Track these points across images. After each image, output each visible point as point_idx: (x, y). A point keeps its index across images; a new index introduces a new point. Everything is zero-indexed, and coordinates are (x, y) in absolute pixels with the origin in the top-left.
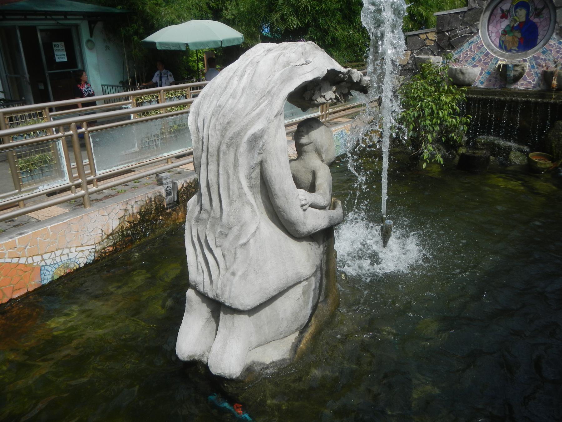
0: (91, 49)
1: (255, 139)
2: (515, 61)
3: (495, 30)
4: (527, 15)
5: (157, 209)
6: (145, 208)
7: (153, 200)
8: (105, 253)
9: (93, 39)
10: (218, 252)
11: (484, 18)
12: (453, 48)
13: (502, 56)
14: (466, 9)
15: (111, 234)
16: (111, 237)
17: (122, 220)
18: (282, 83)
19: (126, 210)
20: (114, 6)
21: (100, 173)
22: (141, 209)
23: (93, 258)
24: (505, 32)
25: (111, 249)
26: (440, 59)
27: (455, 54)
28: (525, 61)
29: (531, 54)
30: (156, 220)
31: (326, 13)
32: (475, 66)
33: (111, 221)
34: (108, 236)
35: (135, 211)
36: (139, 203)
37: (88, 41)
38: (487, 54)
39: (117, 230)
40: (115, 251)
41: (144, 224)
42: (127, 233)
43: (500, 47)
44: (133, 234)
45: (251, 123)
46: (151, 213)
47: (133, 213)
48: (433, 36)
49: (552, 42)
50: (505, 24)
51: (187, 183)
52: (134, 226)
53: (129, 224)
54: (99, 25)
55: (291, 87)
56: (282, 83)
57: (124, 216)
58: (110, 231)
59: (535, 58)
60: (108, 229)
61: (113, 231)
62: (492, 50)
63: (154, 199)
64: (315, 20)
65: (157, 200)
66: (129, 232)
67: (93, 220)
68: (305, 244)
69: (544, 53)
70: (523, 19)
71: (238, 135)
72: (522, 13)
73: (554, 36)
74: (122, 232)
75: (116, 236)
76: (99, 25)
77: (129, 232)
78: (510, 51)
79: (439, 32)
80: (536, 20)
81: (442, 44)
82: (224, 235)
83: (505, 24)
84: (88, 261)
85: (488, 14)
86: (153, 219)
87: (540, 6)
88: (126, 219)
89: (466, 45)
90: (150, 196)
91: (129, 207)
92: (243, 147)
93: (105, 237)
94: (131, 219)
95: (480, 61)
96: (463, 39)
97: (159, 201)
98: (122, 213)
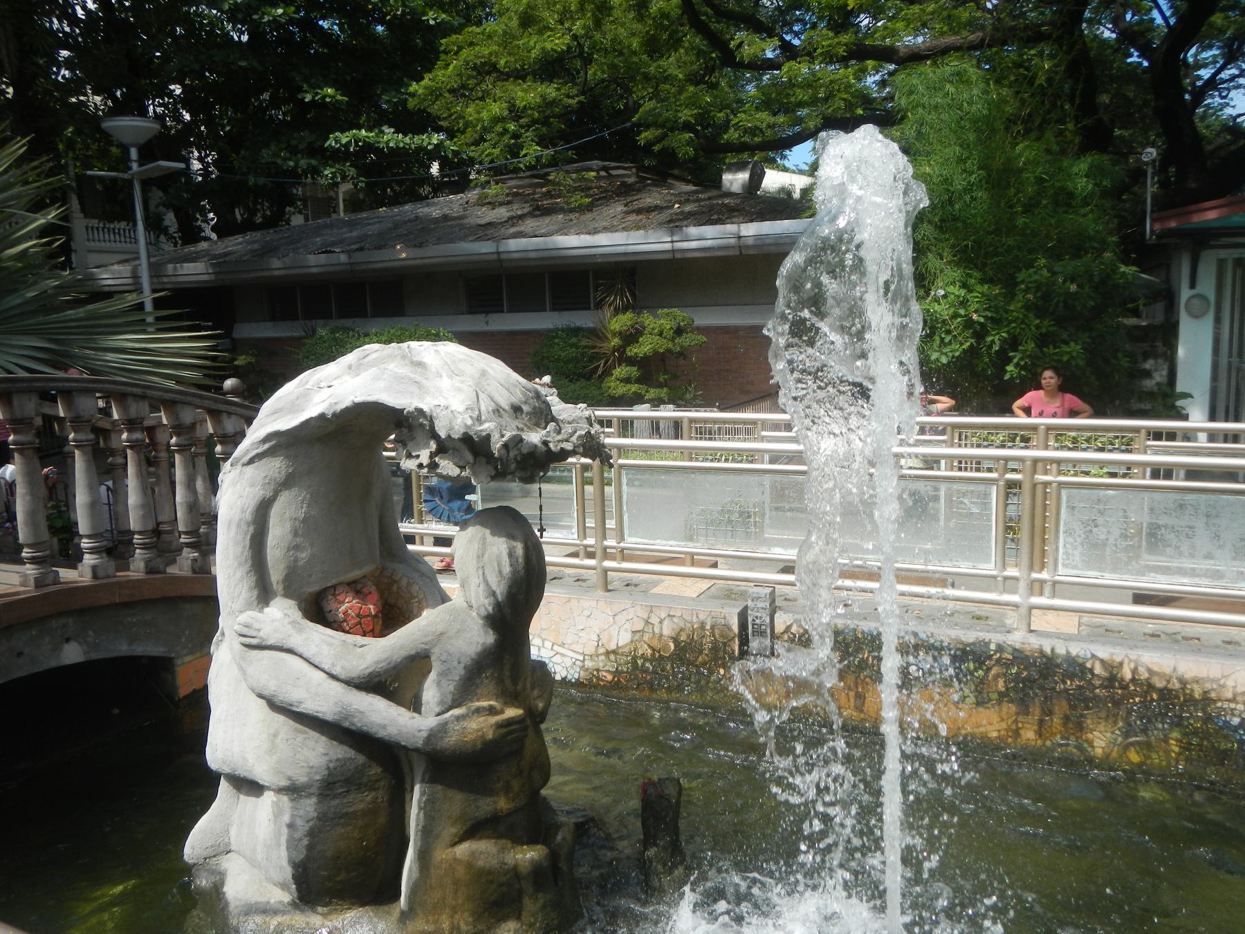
5: (715, 649)
6: (688, 636)
7: (708, 627)
8: (598, 678)
15: (614, 652)
16: (612, 657)
17: (637, 637)
18: (274, 413)
19: (647, 622)
21: (631, 541)
22: (678, 634)
23: (576, 676)
25: (609, 677)
30: (711, 673)
33: (616, 627)
34: (608, 653)
35: (666, 632)
36: (675, 620)
39: (626, 650)
40: (615, 685)
41: (683, 665)
42: (643, 665)
44: (654, 672)
46: (701, 652)
47: (661, 635)
51: (800, 626)
52: (658, 658)
53: (650, 651)
56: (274, 413)
57: (643, 631)
58: (613, 647)
60: (610, 640)
61: (618, 648)
63: (713, 627)
65: (717, 632)
66: (648, 665)
67: (586, 613)
68: (281, 718)
74: (635, 658)
75: (623, 659)
77: (648, 665)
84: (569, 677)
86: (704, 664)
88: (646, 638)
90: (702, 617)
91: (654, 620)
93: (602, 651)
94: (655, 644)
97: (722, 636)
98: (639, 626)
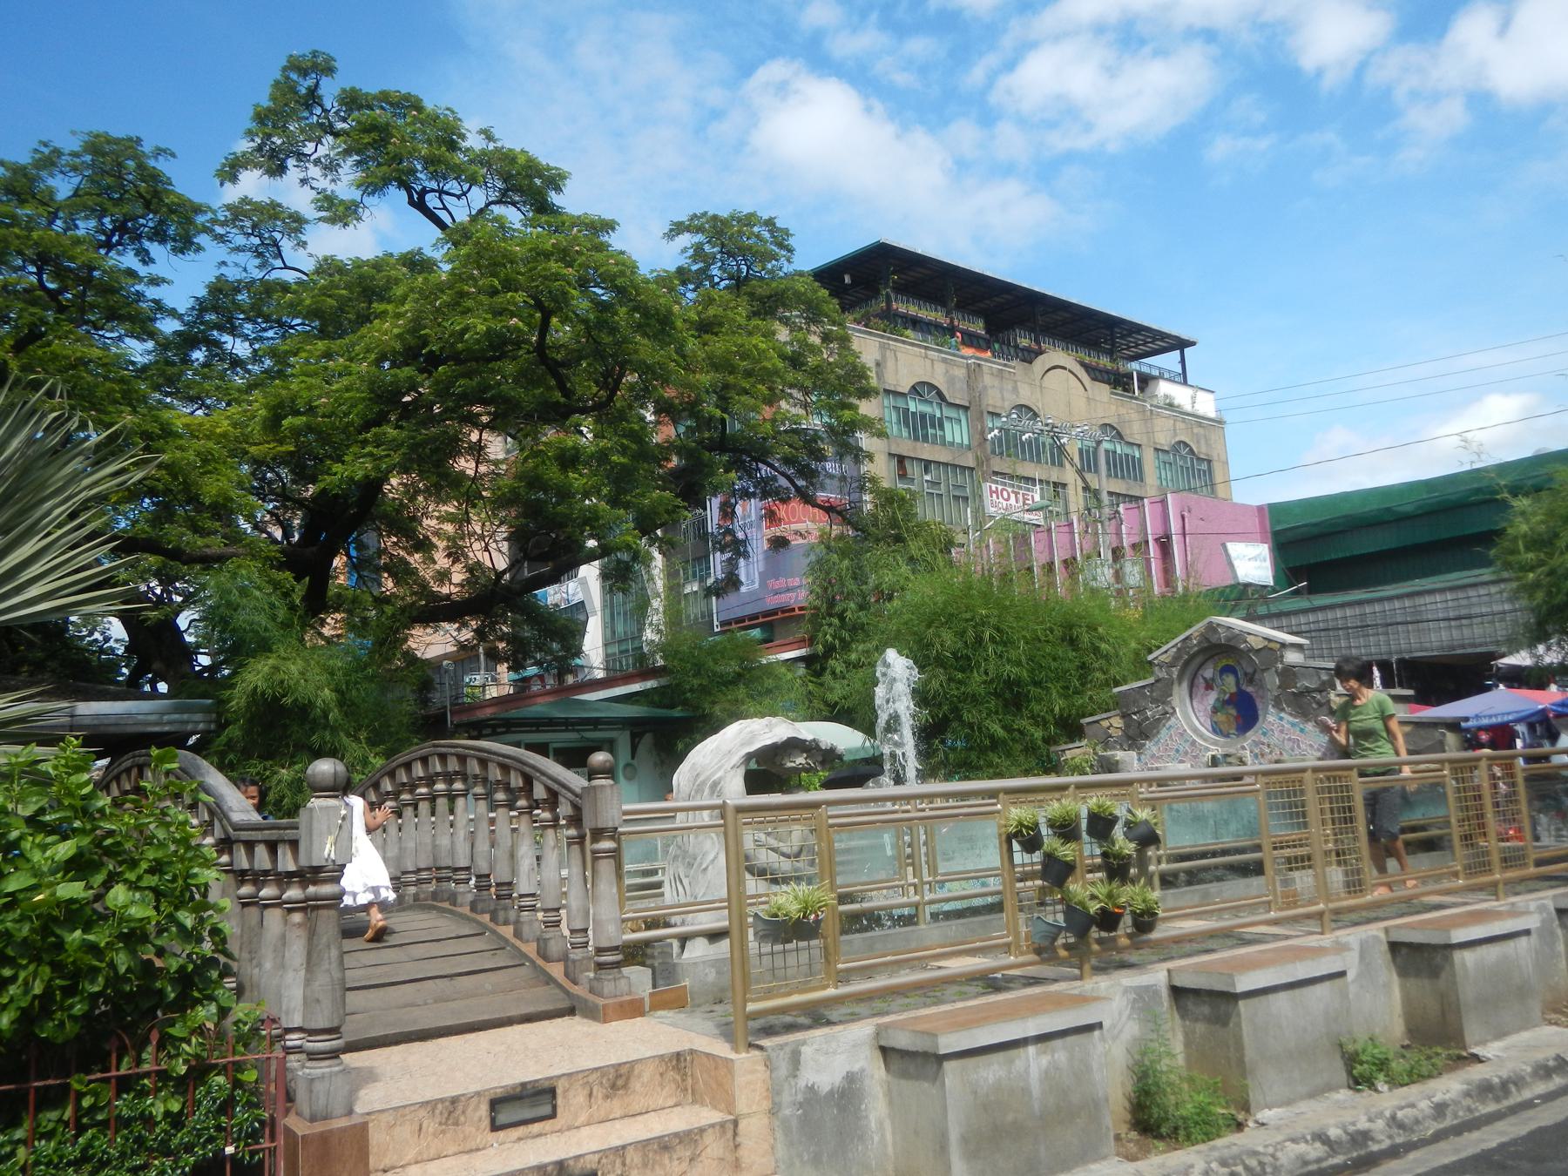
0: (629, 779)
1: (715, 784)
2: (1232, 751)
3: (1202, 707)
4: (1238, 684)
9: (635, 762)
10: (686, 882)
11: (1180, 694)
12: (1147, 738)
13: (1215, 743)
14: (1151, 680)
20: (672, 706)
24: (1215, 710)
26: (1134, 754)
27: (1150, 746)
28: (1243, 748)
29: (1252, 735)
31: (974, 699)
32: (1182, 762)
37: (627, 765)
38: (1194, 742)
43: (1215, 731)
45: (713, 774)
48: (1117, 722)
49: (1270, 718)
50: (1212, 697)
54: (648, 739)
55: (752, 748)
59: (1256, 744)
62: (1201, 736)
64: (956, 710)
69: (1264, 734)
70: (1234, 689)
71: (704, 783)
72: (1230, 680)
73: (1271, 710)
76: (648, 739)
78: (1227, 736)
79: (1124, 716)
80: (1250, 689)
81: (1131, 733)
82: (690, 865)
83: (1212, 697)
85: (1185, 685)
87: (1250, 670)
89: (1164, 732)
92: (707, 791)
95: (1186, 753)
96: (1157, 723)
